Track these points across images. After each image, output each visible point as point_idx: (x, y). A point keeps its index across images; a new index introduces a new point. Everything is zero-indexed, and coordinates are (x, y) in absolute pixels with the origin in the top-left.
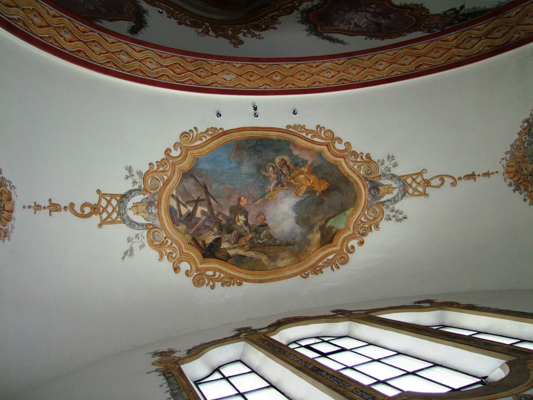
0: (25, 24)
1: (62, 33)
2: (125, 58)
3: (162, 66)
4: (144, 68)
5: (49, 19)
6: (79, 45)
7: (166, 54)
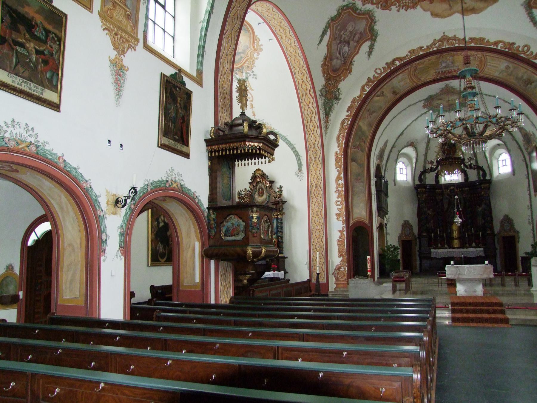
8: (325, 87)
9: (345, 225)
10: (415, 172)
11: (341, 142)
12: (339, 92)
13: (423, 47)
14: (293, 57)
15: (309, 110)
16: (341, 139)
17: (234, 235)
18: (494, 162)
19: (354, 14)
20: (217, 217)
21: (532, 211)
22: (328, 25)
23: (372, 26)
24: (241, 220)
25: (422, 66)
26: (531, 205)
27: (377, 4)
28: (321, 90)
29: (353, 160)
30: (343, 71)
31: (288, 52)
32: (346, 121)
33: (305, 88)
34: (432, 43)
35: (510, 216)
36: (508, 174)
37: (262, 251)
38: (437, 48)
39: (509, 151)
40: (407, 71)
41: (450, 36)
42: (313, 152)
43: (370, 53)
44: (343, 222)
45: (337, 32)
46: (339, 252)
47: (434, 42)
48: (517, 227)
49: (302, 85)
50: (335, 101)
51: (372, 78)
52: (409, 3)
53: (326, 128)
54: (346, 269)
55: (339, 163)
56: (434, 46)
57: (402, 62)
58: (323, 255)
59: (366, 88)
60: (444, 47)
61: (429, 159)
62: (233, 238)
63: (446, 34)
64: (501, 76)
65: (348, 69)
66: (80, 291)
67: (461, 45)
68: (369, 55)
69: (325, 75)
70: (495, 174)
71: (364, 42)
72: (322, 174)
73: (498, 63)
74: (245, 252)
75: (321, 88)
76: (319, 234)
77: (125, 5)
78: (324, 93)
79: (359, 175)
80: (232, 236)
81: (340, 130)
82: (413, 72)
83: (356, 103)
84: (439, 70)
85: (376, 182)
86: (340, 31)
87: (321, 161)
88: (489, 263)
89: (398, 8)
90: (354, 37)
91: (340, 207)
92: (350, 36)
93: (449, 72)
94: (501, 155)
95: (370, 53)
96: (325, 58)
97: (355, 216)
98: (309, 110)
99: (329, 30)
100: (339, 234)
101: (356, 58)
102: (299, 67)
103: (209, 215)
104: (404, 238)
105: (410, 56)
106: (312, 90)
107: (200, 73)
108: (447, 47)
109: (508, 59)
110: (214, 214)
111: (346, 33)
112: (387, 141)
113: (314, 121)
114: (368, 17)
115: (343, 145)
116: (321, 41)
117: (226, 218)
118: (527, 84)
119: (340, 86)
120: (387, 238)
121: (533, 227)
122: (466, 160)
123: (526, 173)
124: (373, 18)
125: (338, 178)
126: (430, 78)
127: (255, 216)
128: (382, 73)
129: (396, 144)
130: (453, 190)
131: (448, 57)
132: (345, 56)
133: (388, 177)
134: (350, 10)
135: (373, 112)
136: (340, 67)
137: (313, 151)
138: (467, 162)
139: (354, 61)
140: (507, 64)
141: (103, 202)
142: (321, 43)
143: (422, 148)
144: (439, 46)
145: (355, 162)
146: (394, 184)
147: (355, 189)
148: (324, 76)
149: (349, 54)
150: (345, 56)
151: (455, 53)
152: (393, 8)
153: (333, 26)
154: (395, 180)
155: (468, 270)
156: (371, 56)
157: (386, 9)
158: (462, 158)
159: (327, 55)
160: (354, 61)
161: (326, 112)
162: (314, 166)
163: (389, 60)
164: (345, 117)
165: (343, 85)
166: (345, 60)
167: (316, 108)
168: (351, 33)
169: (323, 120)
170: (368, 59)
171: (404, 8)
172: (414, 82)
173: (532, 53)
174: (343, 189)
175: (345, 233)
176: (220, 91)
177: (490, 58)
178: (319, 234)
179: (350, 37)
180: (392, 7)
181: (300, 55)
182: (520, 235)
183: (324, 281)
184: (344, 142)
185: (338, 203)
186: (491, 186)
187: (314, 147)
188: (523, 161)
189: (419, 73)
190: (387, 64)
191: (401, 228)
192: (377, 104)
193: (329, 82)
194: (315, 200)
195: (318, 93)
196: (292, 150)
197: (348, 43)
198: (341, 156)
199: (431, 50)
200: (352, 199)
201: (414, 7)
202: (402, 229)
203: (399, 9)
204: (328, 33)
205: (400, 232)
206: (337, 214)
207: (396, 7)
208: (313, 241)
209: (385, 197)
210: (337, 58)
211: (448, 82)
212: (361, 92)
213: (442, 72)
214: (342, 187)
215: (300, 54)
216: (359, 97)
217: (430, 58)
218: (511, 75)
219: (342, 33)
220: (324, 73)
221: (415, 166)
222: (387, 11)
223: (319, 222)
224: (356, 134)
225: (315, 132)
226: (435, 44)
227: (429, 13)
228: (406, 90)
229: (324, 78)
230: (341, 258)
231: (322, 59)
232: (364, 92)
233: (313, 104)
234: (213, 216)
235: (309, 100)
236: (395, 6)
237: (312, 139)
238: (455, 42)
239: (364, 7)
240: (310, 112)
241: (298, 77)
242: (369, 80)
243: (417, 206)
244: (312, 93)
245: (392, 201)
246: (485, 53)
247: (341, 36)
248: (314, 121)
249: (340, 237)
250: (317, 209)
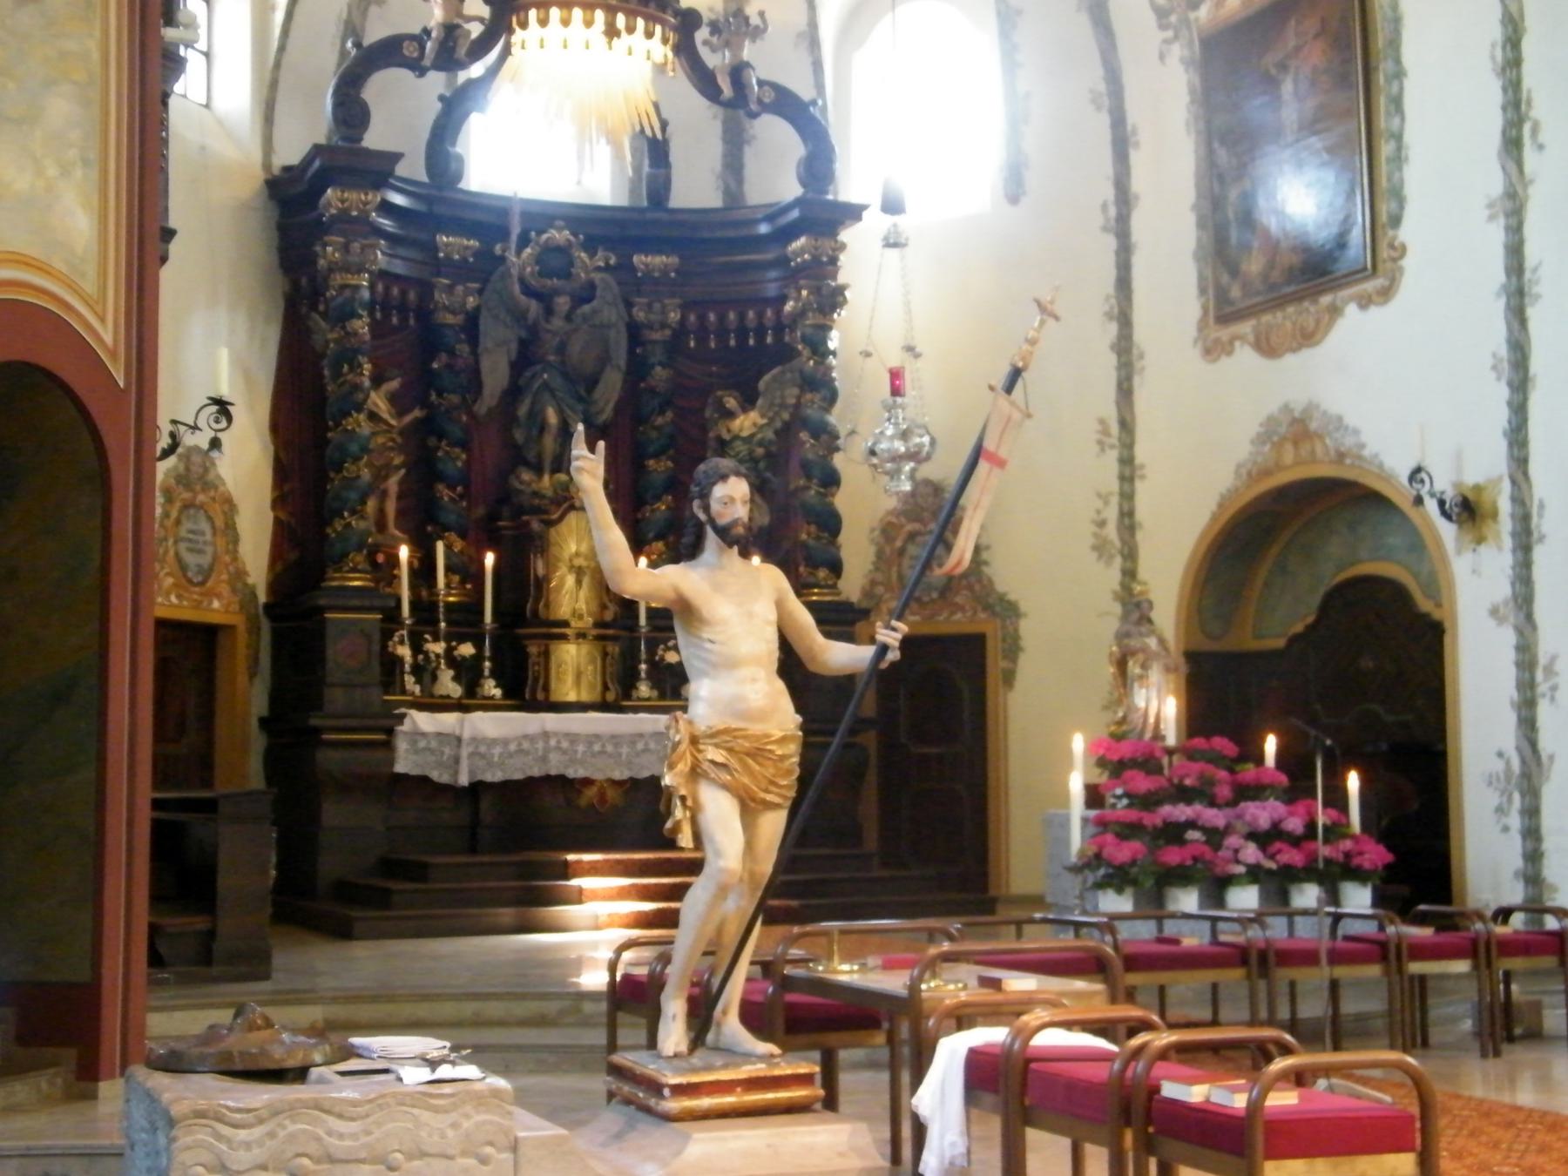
10: (282, 48)
21: (1127, 461)
26: (1127, 425)
130: (563, 250)
182: (1025, 627)
188: (1095, 100)
243: (272, 335)
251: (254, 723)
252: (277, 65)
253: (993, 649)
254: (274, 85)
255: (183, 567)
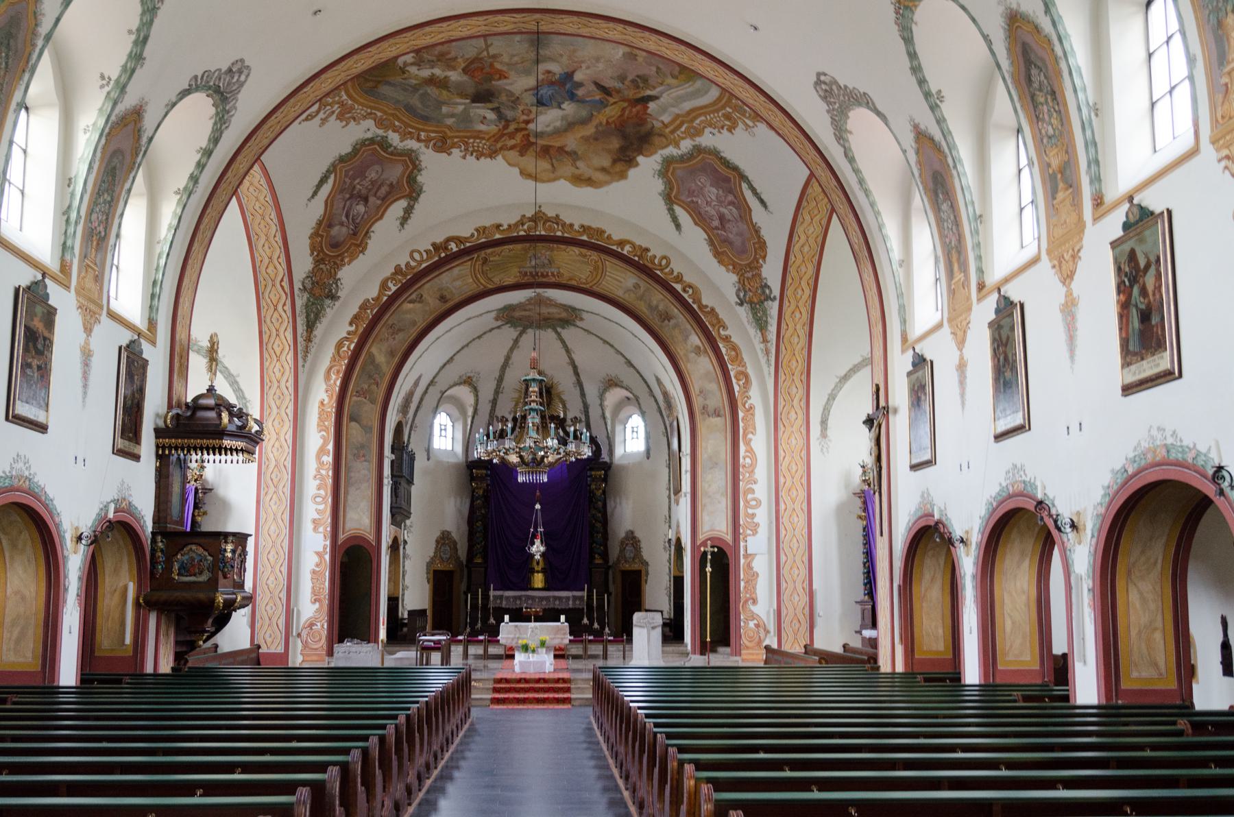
0: (804, 325)
1: (799, 296)
2: (806, 249)
3: (812, 222)
4: (814, 235)
5: (793, 307)
6: (804, 284)
7: (800, 218)
8: (312, 275)
9: (328, 543)
10: (470, 434)
11: (332, 382)
12: (337, 286)
13: (501, 225)
14: (258, 218)
15: (276, 315)
16: (334, 377)
17: (195, 575)
18: (619, 428)
19: (382, 153)
20: (167, 546)
22: (331, 169)
23: (414, 175)
24: (207, 554)
25: (497, 258)
26: (670, 517)
27: (427, 141)
28: (304, 279)
29: (353, 419)
30: (349, 248)
31: (251, 208)
32: (347, 343)
33: (272, 276)
34: (518, 222)
35: (638, 534)
36: (639, 453)
37: (237, 598)
38: (525, 231)
39: (643, 414)
40: (470, 263)
41: (549, 215)
42: (276, 397)
43: (404, 220)
44: (325, 536)
45: (347, 180)
46: (314, 592)
47: (521, 219)
48: (646, 555)
49: (267, 268)
50: (328, 302)
51: (403, 267)
52: (483, 148)
53: (306, 351)
54: (325, 626)
55: (326, 423)
56: (521, 227)
57: (462, 247)
58: (280, 599)
59: (390, 285)
60: (538, 233)
61: (499, 413)
62: (192, 579)
63: (543, 209)
64: (626, 296)
65: (359, 246)
66: (33, 652)
67: (566, 235)
68: (402, 224)
69: (315, 253)
70: (619, 451)
71: (395, 201)
72: (290, 442)
73: (623, 275)
74: (213, 601)
75: (305, 276)
76: (276, 557)
77: (95, 264)
78: (309, 286)
79: (362, 447)
80: (191, 576)
81: (333, 359)
82: (480, 267)
83: (369, 311)
84: (525, 270)
85: (392, 462)
86: (353, 178)
87: (289, 414)
88: (567, 620)
89: (464, 153)
90: (379, 189)
91: (321, 507)
92: (369, 187)
93: (543, 276)
94: (631, 416)
95: (404, 220)
96: (320, 223)
97: (349, 525)
98: (276, 315)
99: (332, 176)
100: (316, 559)
101: (378, 227)
102: (266, 235)
103: (154, 541)
104: (439, 567)
105: (478, 239)
106: (286, 279)
107: (152, 324)
108: (543, 233)
109: (639, 274)
110: (162, 541)
111: (364, 183)
112: (420, 377)
113: (282, 337)
114: (410, 169)
115: (337, 389)
116: (315, 193)
117: (183, 549)
118: (664, 320)
119: (340, 274)
120: (404, 567)
121: (670, 555)
122: (569, 422)
123: (667, 458)
124: (417, 162)
125: (322, 451)
126: (509, 281)
127: (229, 547)
128: (422, 261)
129: (436, 380)
131: (543, 251)
132: (358, 221)
133: (415, 446)
134: (376, 146)
135: (400, 330)
136: (343, 242)
137: (275, 394)
138: (570, 426)
139: (373, 232)
140: (635, 281)
141: (68, 537)
142: (316, 197)
143: (487, 392)
144: (529, 228)
145: (356, 421)
146: (426, 457)
147: (352, 474)
148: (312, 254)
149: (366, 217)
150: (358, 221)
151: (555, 246)
152: (455, 151)
153: (341, 171)
154: (428, 450)
155: (532, 631)
156: (405, 226)
157: (442, 152)
158: (562, 416)
159: (323, 219)
160: (373, 232)
161: (308, 321)
162: (276, 423)
163: (439, 239)
164: (345, 335)
165: (349, 274)
166: (356, 227)
167: (289, 313)
168: (373, 182)
169: (302, 337)
170: (400, 230)
171: (474, 154)
172: (482, 284)
173: (672, 271)
174: (330, 473)
175: (327, 557)
176: (177, 349)
177: (611, 265)
178: (276, 557)
179: (370, 190)
180: (454, 150)
181: (272, 217)
183: (281, 649)
184: (338, 383)
185: (319, 500)
186: (610, 473)
187: (279, 387)
189: (490, 269)
190: (434, 245)
191: (434, 546)
192: (408, 316)
193: (322, 266)
194: (272, 489)
195: (297, 285)
196: (230, 385)
197: (366, 200)
198: (331, 409)
199: (516, 234)
200: (346, 493)
201: (492, 154)
202: (437, 546)
203: (465, 155)
204: (331, 181)
205: (432, 554)
206: (314, 521)
207: (461, 151)
208: (262, 570)
209: (406, 486)
210: (342, 224)
211: (538, 290)
212: (380, 290)
213: (531, 273)
214: (327, 470)
215: (274, 215)
216: (377, 299)
217: (511, 247)
218: (641, 298)
219: (357, 181)
220: (313, 248)
221: (472, 422)
222: (445, 154)
223: (277, 531)
224: (363, 369)
225: (283, 358)
226: (523, 224)
227: (516, 170)
228: (464, 297)
229: (311, 259)
230: (317, 605)
231: (314, 225)
232: (387, 293)
233: (284, 305)
234: (160, 544)
235: (278, 296)
236: (458, 150)
237: (276, 370)
238: (556, 227)
239: (401, 144)
240: (278, 320)
241: (263, 253)
242: (398, 270)
244: (286, 284)
245: (418, 491)
246: (603, 256)
247: (354, 187)
248: (282, 337)
249: (317, 565)
250: (274, 508)
251: (462, 593)
252: (469, 438)
253: (643, 573)
254: (468, 442)
255: (442, 558)
